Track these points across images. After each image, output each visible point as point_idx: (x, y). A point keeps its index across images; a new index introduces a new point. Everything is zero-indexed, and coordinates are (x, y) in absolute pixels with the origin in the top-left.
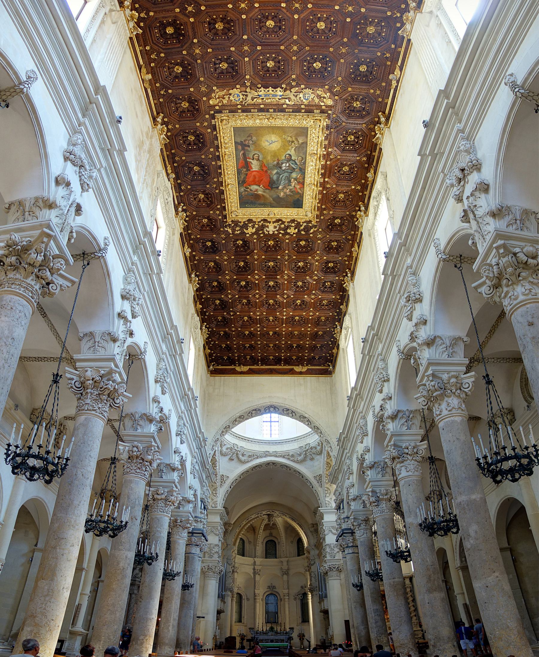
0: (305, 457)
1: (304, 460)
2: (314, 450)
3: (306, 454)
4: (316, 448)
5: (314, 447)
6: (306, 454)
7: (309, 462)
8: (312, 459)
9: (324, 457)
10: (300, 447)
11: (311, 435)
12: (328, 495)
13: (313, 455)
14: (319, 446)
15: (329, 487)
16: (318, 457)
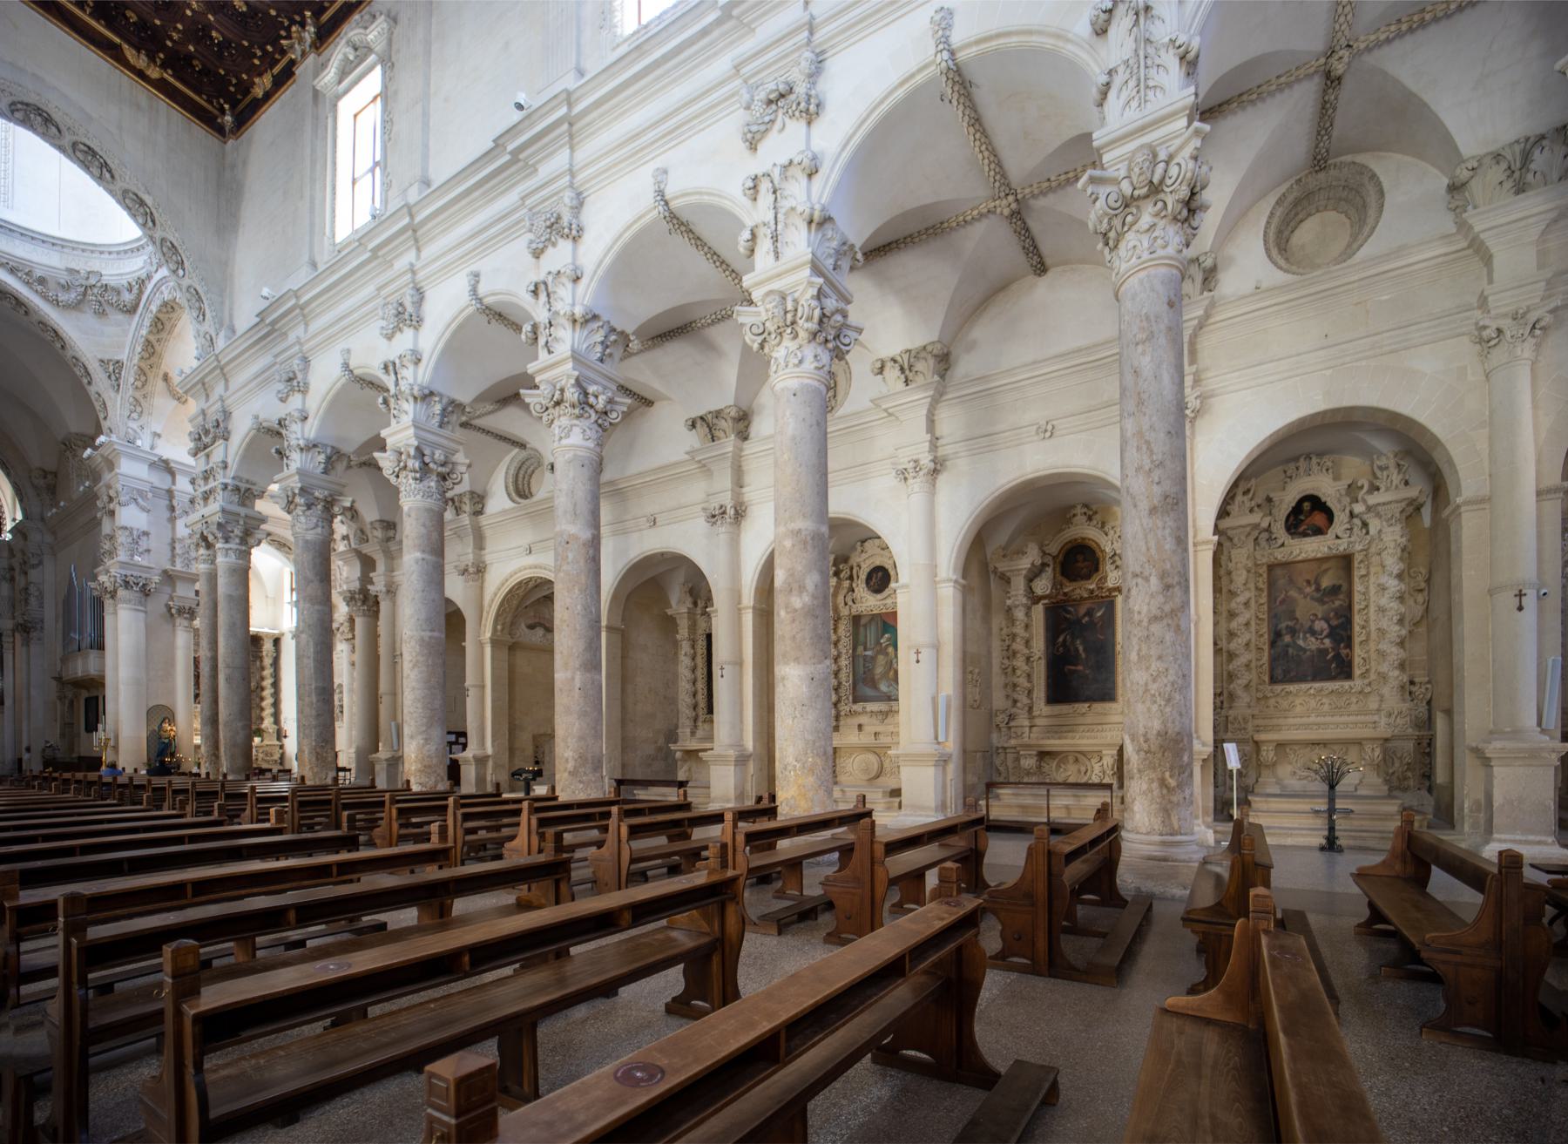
0: (80, 302)
1: (76, 306)
2: (109, 296)
3: (85, 294)
4: (119, 293)
5: (113, 289)
6: (85, 294)
7: (88, 319)
8: (101, 314)
9: (140, 326)
10: (71, 271)
11: (106, 256)
12: (135, 415)
13: (108, 309)
14: (130, 291)
15: (141, 400)
16: (120, 317)
